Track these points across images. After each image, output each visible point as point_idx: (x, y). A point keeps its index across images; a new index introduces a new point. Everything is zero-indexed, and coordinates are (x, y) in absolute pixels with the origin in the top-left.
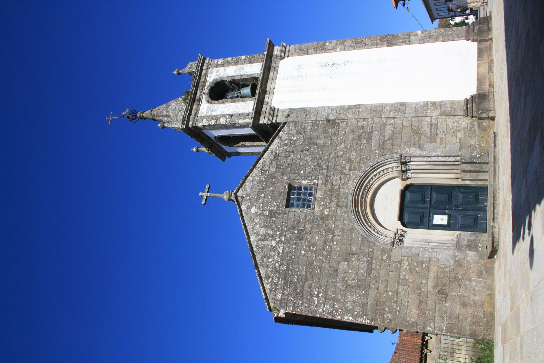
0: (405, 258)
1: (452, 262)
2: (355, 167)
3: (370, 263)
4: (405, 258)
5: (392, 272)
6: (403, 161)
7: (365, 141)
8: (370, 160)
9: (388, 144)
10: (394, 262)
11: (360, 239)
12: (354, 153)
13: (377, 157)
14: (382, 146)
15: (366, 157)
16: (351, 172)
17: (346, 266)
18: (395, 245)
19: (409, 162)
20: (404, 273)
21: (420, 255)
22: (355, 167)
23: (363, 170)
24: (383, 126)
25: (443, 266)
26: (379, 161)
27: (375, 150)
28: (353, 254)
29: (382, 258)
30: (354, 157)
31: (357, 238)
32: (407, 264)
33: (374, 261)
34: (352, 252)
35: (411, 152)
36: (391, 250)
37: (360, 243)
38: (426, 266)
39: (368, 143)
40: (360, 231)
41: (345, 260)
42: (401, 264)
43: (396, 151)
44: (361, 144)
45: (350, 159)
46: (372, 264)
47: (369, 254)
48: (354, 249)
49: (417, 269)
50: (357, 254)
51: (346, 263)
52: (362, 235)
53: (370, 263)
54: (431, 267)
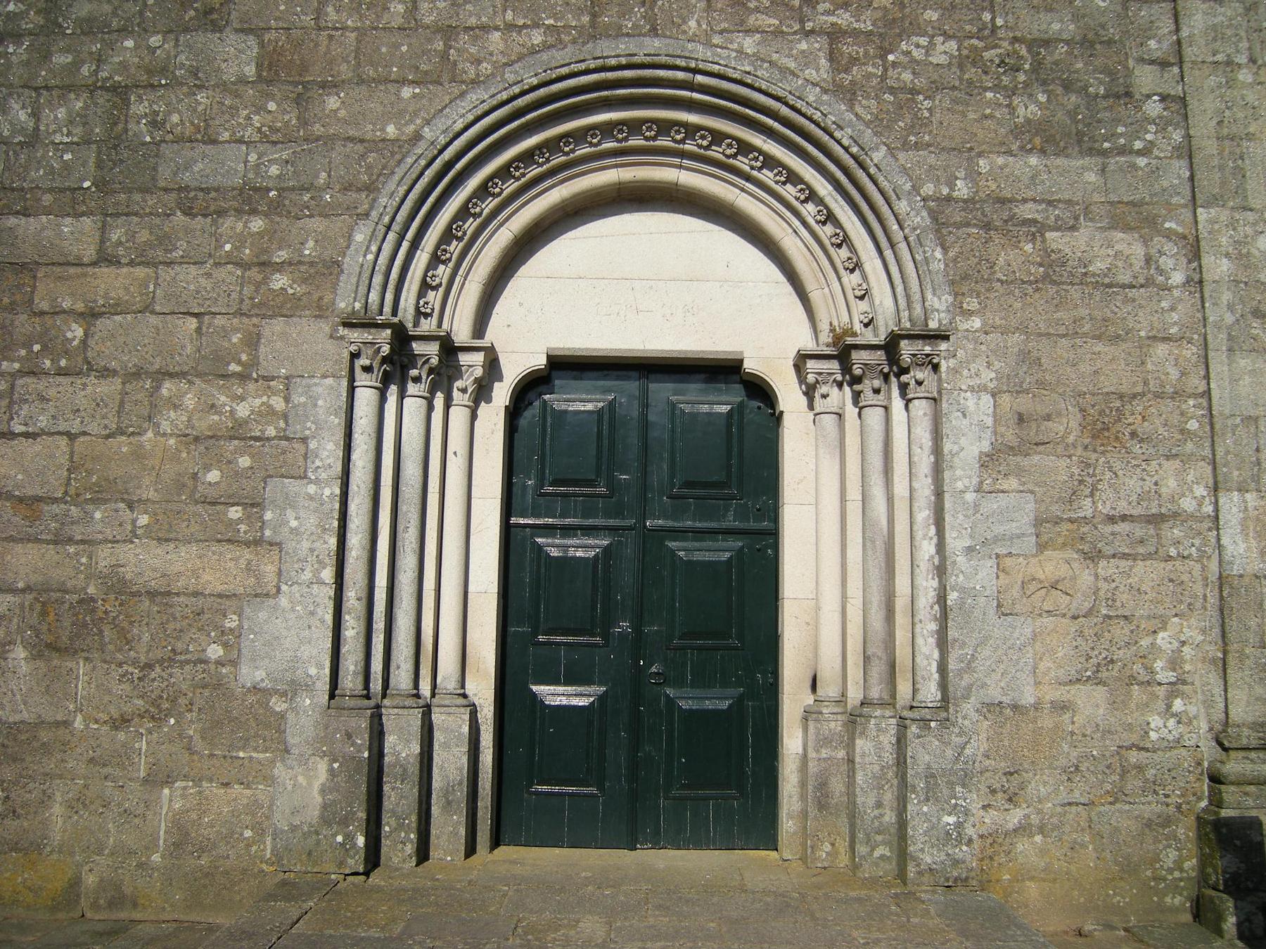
0: (278, 403)
1: (260, 674)
2: (854, 61)
3: (250, 198)
4: (278, 403)
5: (198, 330)
6: (907, 349)
7: (1027, 110)
8: (906, 146)
9: (1013, 258)
10: (253, 341)
11: (391, 130)
12: (945, 50)
13: (928, 189)
14: (993, 216)
15: (919, 124)
16: (819, 43)
17: (230, 73)
18: (355, 335)
19: (903, 388)
20: (190, 401)
21: (293, 486)
22: (854, 61)
23: (835, 111)
24: (1136, 217)
25: (231, 622)
26: (902, 206)
27: (973, 175)
28: (298, 100)
29: (279, 267)
30: (917, 54)
31: (398, 115)
32: (243, 410)
33: (257, 224)
34: (316, 92)
35: (970, 401)
36: (321, 311)
37: (368, 131)
38: (232, 524)
39: (1017, 132)
40: (441, 123)
41: (272, 69)
42: (243, 377)
43: (972, 303)
44: (1012, 92)
45: (903, 34)
46: (239, 212)
47: (303, 189)
48: (333, 102)
49: (213, 476)
50: (303, 122)
51: (250, 71)
52: (417, 137)
53: (250, 198)
54: (229, 552)
